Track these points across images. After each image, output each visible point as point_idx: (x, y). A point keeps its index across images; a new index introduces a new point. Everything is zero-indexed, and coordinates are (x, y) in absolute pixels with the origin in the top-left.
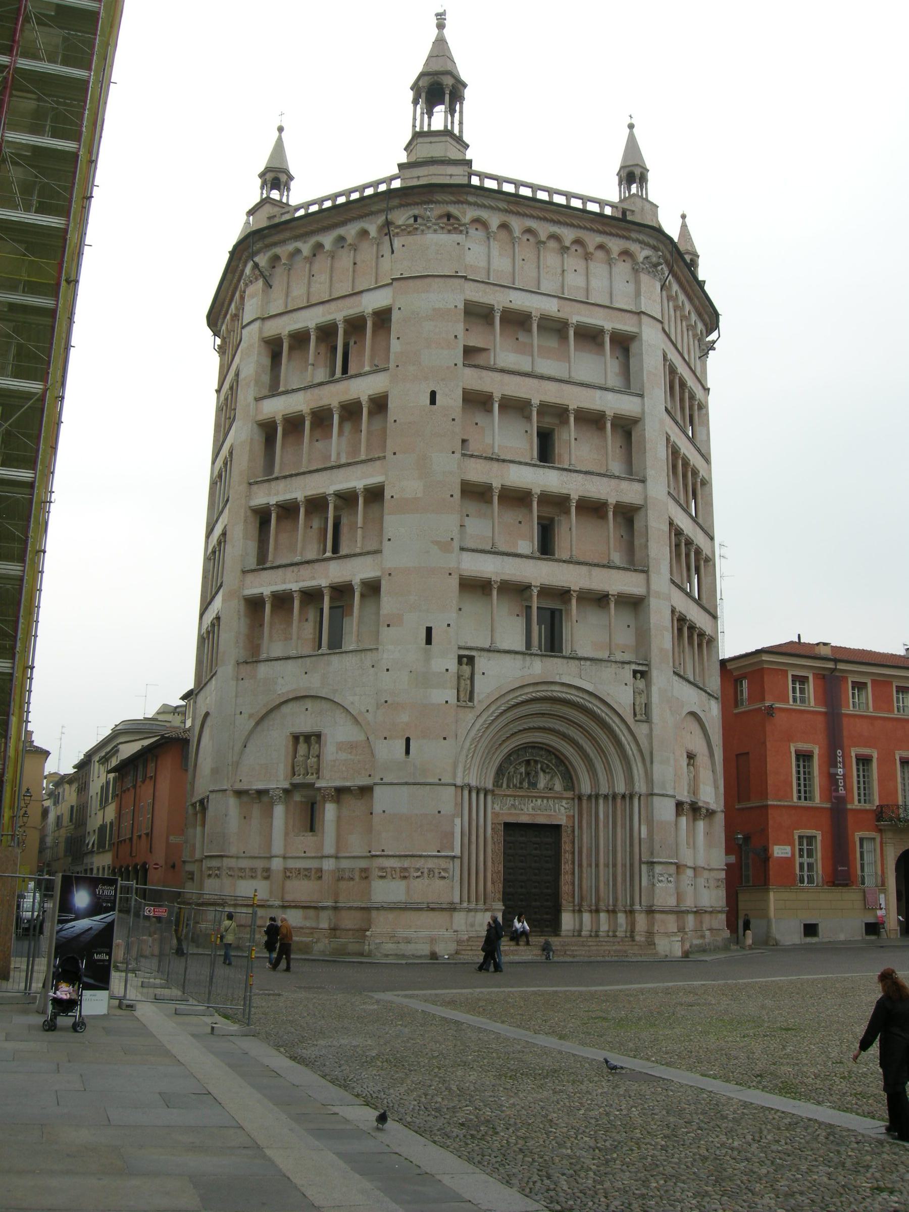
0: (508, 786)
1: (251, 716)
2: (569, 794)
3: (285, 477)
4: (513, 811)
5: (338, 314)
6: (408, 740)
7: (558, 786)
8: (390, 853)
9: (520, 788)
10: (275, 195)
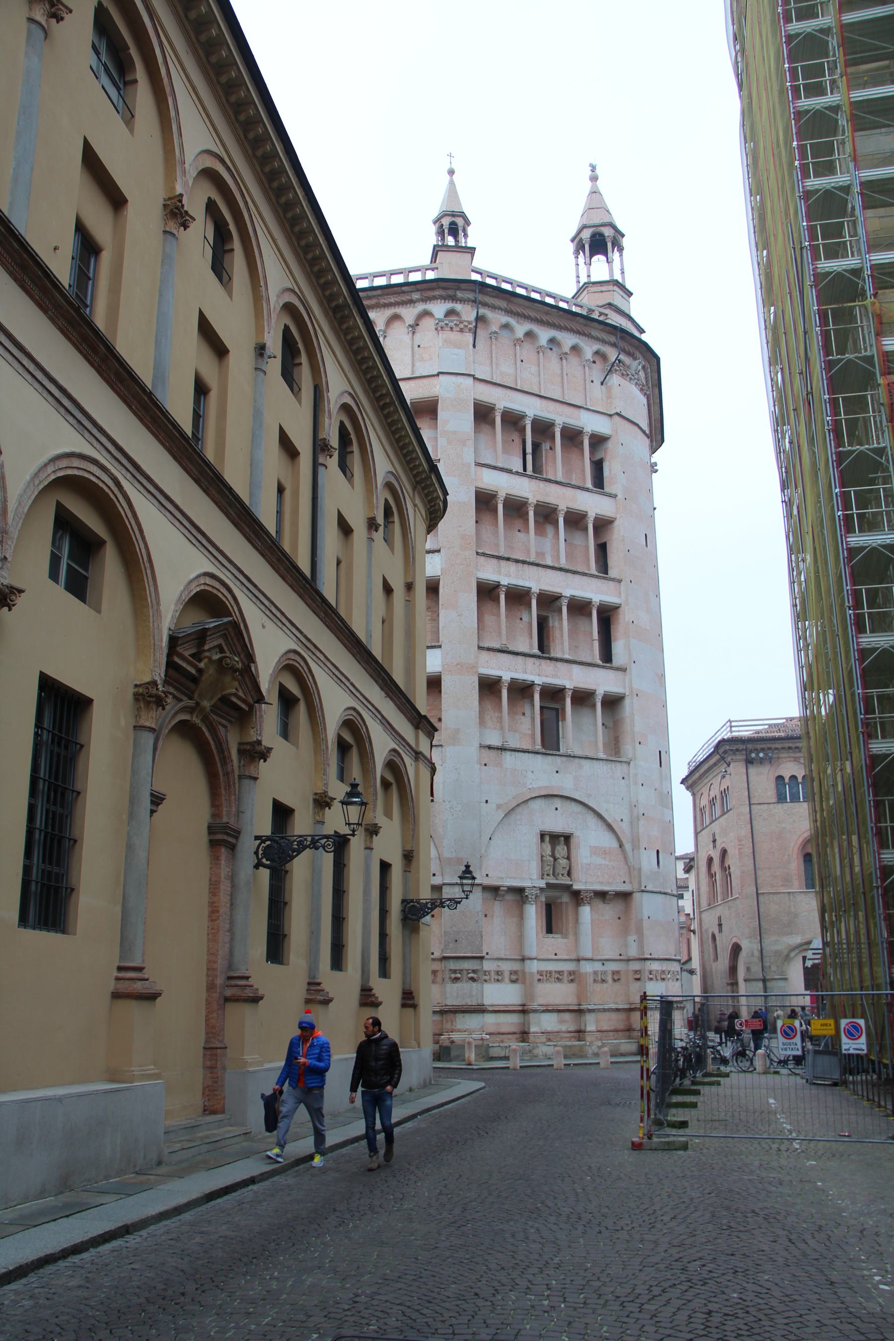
1: (499, 807)
3: (517, 561)
5: (560, 417)
6: (658, 852)
8: (656, 957)
10: (450, 241)
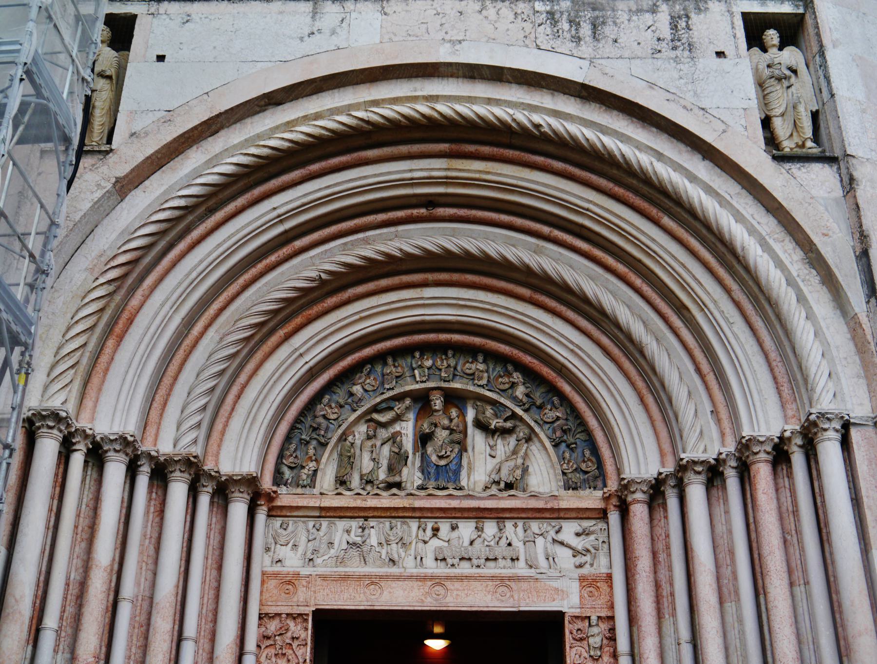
0: (342, 482)
2: (591, 499)
4: (355, 567)
7: (543, 475)
9: (389, 486)
